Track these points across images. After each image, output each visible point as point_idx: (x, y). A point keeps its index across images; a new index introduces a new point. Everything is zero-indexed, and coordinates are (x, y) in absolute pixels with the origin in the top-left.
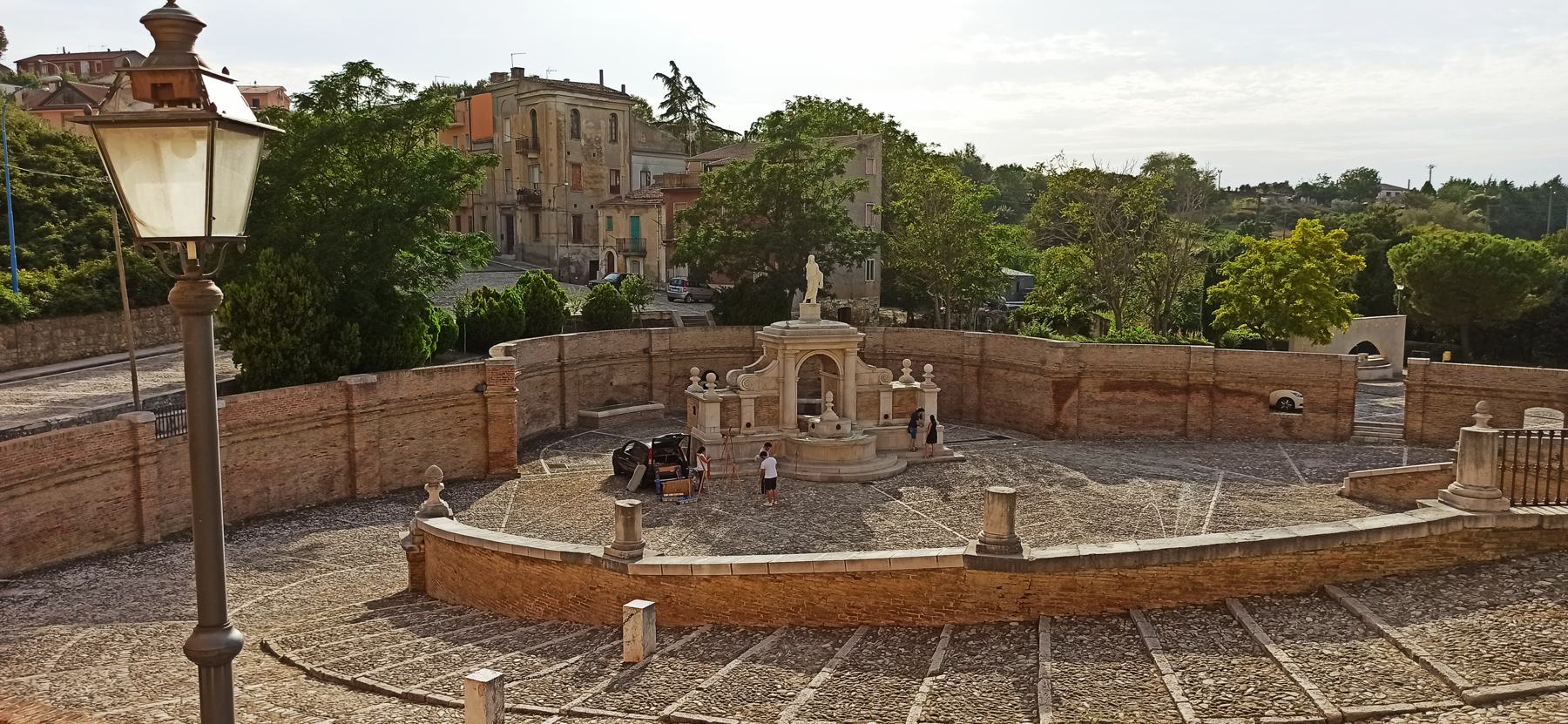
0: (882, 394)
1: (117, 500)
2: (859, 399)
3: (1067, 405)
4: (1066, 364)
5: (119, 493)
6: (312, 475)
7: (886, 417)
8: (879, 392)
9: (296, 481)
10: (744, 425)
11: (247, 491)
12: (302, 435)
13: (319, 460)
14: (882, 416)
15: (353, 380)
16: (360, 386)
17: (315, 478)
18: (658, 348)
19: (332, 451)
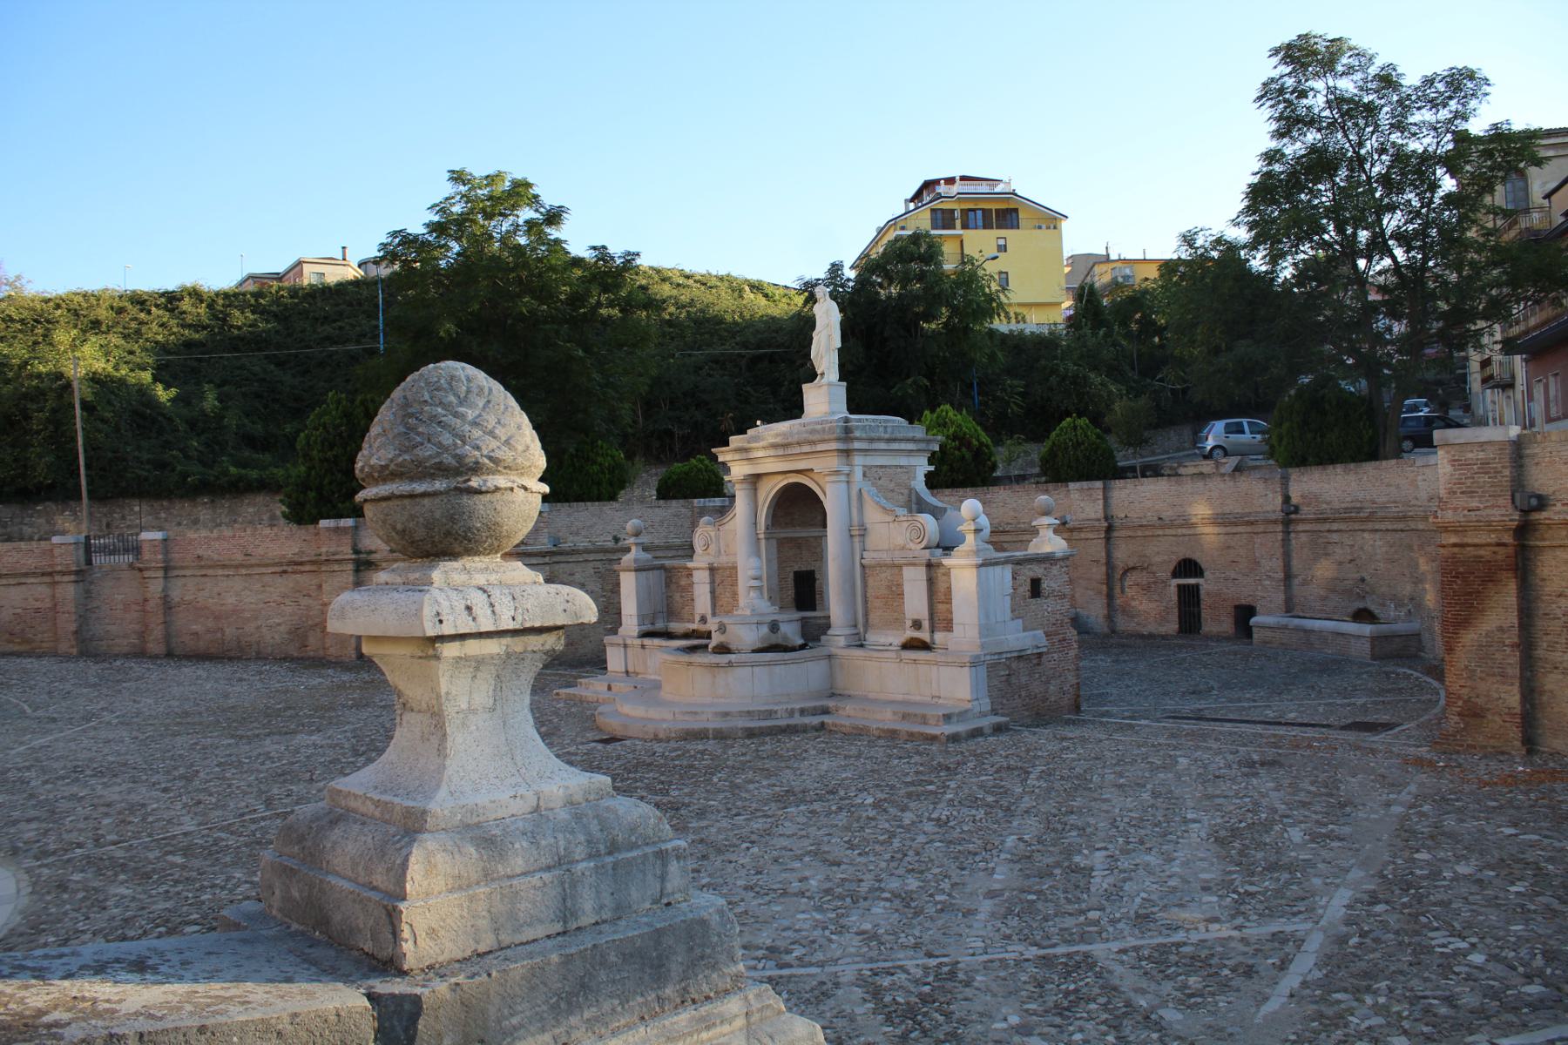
0: (908, 573)
1: (37, 610)
2: (871, 582)
3: (1469, 637)
4: (1462, 501)
5: (38, 604)
6: (279, 624)
7: (917, 625)
8: (900, 567)
9: (258, 628)
10: (697, 618)
11: (195, 627)
12: (267, 579)
13: (288, 610)
14: (909, 623)
15: (324, 523)
16: (328, 529)
17: (282, 628)
18: (1083, 516)
19: (305, 601)
